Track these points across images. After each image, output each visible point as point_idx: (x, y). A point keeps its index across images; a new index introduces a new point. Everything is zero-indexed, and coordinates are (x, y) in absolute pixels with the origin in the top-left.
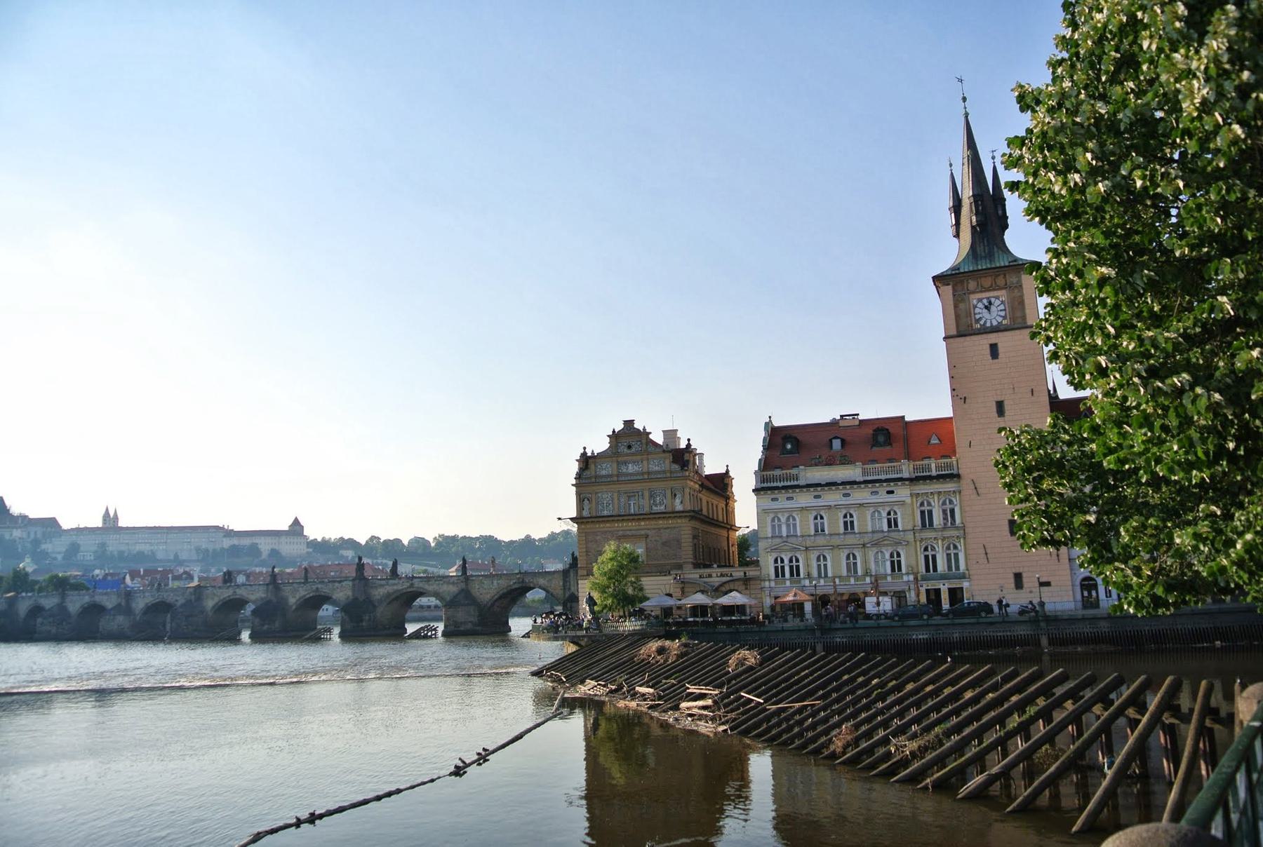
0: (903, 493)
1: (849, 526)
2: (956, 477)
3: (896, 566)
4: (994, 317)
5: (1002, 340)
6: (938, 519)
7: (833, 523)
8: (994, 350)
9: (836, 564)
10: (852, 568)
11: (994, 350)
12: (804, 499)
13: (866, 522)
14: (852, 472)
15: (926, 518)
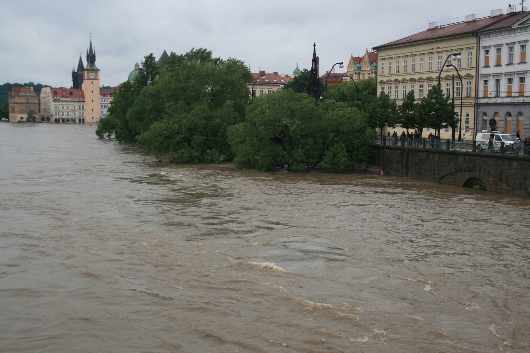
0: (76, 103)
1: (68, 108)
2: (84, 101)
3: (75, 115)
4: (92, 77)
5: (94, 81)
6: (81, 108)
7: (65, 107)
8: (92, 83)
9: (65, 114)
10: (68, 115)
11: (92, 83)
12: (61, 103)
13: (70, 107)
14: (69, 99)
15: (80, 107)
